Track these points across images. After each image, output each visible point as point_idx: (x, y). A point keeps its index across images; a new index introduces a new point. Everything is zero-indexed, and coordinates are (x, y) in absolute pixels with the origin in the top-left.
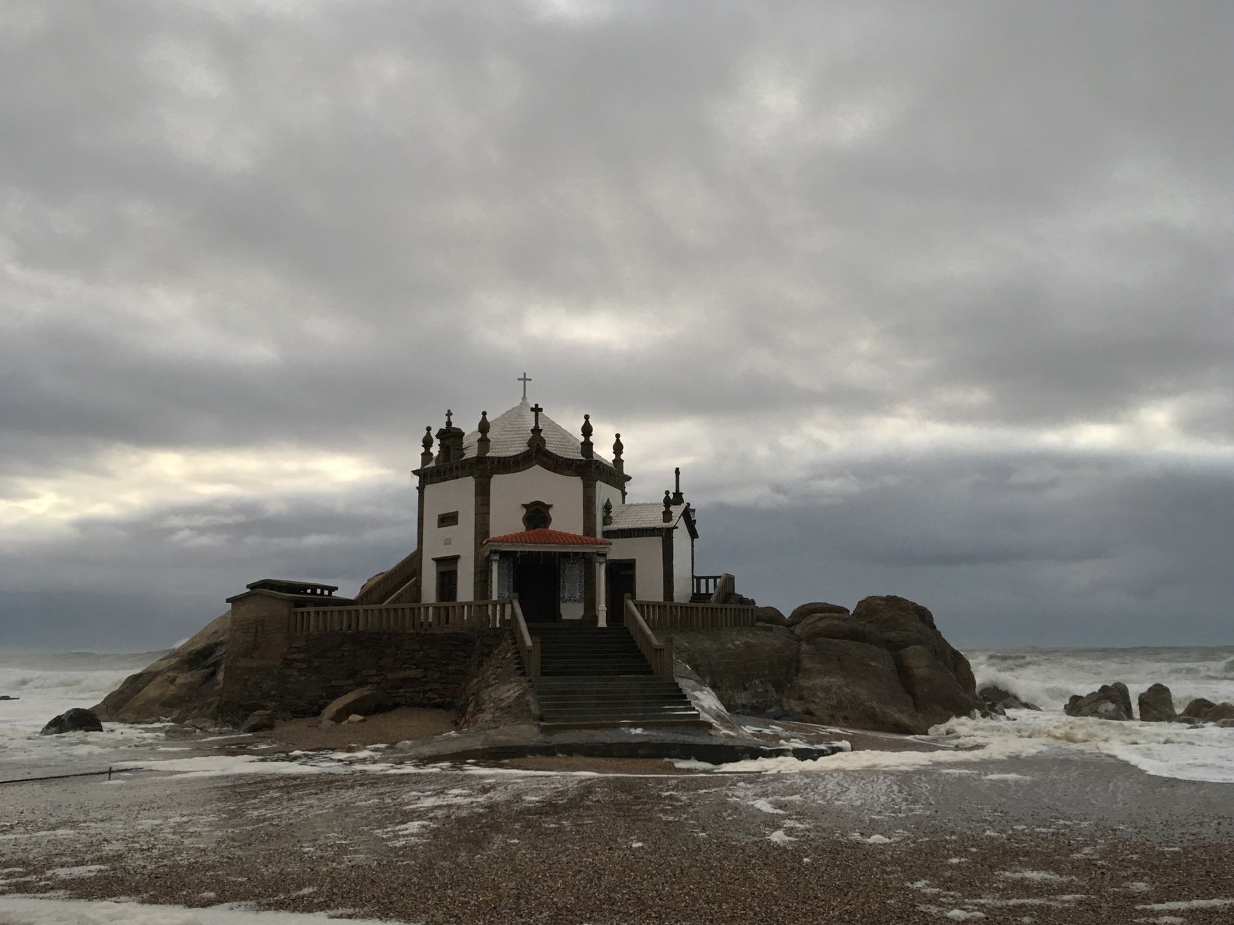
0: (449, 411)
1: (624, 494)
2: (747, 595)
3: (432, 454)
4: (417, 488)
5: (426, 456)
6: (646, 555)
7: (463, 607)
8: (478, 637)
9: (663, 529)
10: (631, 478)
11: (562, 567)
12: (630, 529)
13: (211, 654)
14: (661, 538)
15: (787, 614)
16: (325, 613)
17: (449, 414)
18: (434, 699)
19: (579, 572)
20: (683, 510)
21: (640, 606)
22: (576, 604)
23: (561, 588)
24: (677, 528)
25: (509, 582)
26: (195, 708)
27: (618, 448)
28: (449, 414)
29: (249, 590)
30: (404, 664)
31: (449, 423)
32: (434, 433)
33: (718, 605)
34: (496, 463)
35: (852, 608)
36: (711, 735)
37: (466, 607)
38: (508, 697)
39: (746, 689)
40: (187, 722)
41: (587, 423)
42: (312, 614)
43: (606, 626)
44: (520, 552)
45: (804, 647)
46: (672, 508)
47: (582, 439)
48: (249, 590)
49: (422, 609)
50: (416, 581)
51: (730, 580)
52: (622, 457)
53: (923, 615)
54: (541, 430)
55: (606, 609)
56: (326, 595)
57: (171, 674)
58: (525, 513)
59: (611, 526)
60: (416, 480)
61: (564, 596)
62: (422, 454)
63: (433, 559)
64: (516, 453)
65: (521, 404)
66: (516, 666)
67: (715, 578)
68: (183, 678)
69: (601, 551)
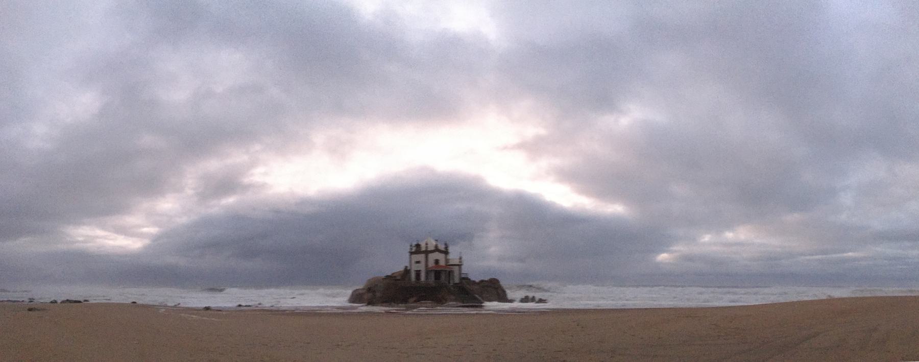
5: (411, 249)
6: (456, 269)
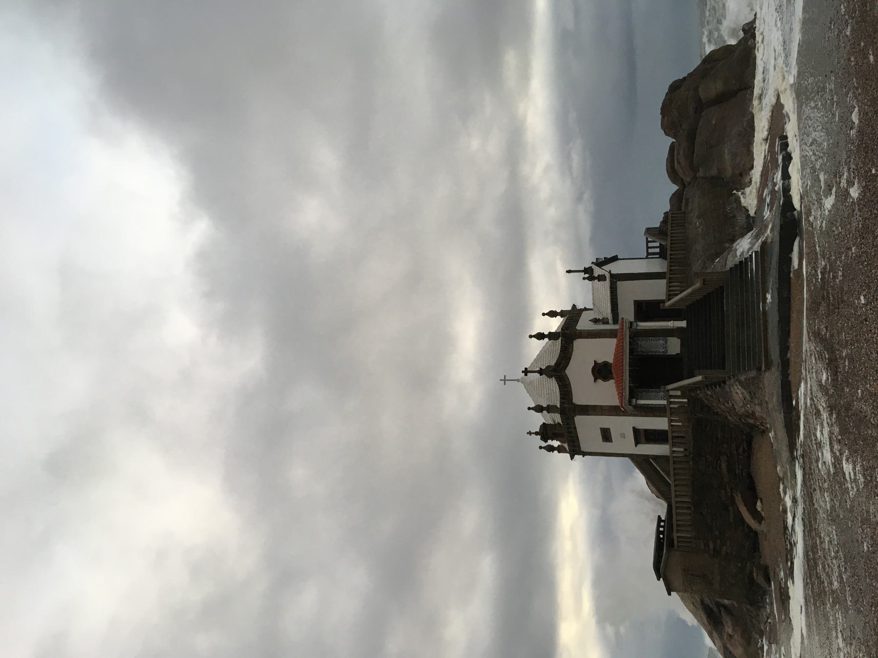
0: (528, 433)
1: (585, 309)
2: (661, 218)
3: (559, 445)
4: (583, 456)
5: (560, 450)
6: (631, 292)
7: (672, 425)
8: (695, 415)
9: (611, 281)
10: (574, 305)
11: (640, 353)
12: (612, 305)
13: (711, 609)
14: (618, 282)
15: (675, 188)
16: (678, 525)
17: (530, 433)
18: (744, 448)
19: (644, 341)
20: (596, 267)
21: (670, 296)
22: (668, 343)
23: (657, 354)
24: (610, 271)
25: (652, 392)
26: (752, 621)
27: (552, 314)
28: (530, 433)
29: (661, 579)
30: (717, 469)
31: (537, 433)
32: (544, 444)
33: (669, 239)
34: (564, 401)
35: (672, 140)
36: (772, 242)
37: (672, 424)
38: (742, 393)
39: (735, 216)
40: (763, 628)
41: (534, 336)
42: (679, 534)
43: (686, 321)
44: (629, 384)
45: (700, 174)
46: (596, 275)
47: (546, 340)
48: (661, 579)
49: (674, 455)
50: (652, 459)
51: (649, 231)
52: (558, 311)
53: (675, 87)
54: (540, 368)
55: (672, 321)
56: (665, 524)
57: (725, 638)
58: (600, 380)
59: (609, 318)
60: (578, 457)
61: (662, 352)
62: (559, 452)
63: (636, 446)
64: (558, 387)
65: (522, 382)
66: (718, 387)
67: (648, 242)
68: (729, 630)
69: (628, 325)
